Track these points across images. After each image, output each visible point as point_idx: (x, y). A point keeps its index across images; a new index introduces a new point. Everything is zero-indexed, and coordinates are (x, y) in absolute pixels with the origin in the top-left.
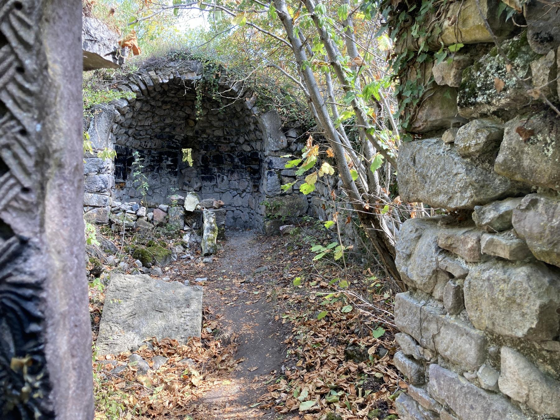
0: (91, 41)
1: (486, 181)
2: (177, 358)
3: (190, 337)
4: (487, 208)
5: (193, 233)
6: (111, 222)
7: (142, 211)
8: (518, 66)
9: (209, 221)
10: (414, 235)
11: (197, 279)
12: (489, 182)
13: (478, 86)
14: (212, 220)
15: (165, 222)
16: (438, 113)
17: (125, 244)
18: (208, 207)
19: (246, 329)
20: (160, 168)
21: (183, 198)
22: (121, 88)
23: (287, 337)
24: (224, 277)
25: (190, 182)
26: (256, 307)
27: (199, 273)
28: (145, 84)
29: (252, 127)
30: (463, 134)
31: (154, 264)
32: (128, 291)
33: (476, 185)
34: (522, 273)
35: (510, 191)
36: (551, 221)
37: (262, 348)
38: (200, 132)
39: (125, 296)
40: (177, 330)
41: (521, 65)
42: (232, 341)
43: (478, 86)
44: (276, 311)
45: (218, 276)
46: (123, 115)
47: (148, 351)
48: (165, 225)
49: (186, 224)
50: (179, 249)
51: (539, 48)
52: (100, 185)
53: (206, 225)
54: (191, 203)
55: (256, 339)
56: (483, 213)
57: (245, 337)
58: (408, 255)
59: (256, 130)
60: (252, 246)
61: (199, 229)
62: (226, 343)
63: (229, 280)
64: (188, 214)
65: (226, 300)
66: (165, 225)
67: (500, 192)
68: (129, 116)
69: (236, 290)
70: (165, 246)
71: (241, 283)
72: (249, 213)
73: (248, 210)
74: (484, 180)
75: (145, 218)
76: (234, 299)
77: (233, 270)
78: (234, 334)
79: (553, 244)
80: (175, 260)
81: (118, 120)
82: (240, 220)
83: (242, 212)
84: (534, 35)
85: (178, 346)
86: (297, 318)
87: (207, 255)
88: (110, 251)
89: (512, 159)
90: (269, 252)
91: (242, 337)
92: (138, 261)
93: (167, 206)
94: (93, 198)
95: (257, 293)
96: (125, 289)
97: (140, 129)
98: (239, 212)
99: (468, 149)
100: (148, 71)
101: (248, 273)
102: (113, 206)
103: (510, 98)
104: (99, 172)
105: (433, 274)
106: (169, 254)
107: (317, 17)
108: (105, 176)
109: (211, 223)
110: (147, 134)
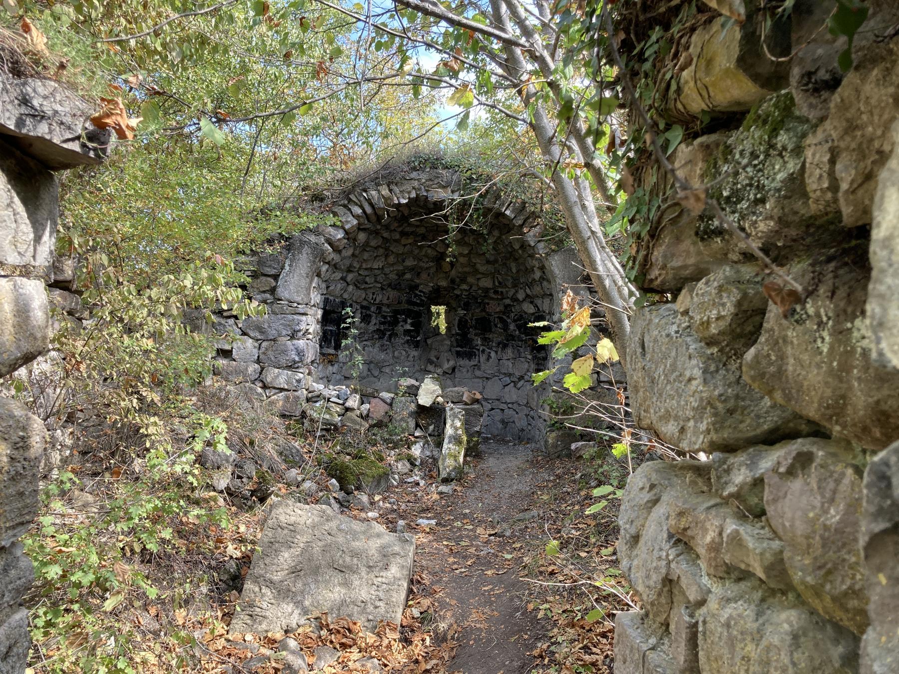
0: (34, 116)
1: (743, 399)
2: (355, 654)
3: (382, 621)
4: (740, 458)
5: (427, 442)
6: (304, 415)
7: (353, 402)
8: (784, 148)
9: (453, 426)
10: (646, 496)
11: (420, 521)
12: (748, 402)
13: (725, 194)
14: (458, 424)
15: (386, 420)
16: (688, 252)
17: (318, 451)
18: (455, 401)
19: (476, 619)
20: (394, 335)
21: (417, 384)
22: (336, 210)
23: (539, 645)
24: (465, 521)
25: (438, 359)
26: (501, 582)
27: (427, 510)
28: (371, 204)
29: (537, 275)
30: (703, 295)
31: (358, 488)
32: (294, 531)
33: (720, 406)
34: (786, 626)
35: (791, 425)
36: (826, 512)
37: (495, 659)
38: (458, 280)
39: (290, 539)
40: (363, 605)
41: (790, 147)
42: (449, 637)
43: (725, 194)
44: (531, 594)
45: (456, 519)
46: (336, 250)
47: (312, 635)
48: (386, 426)
49: (417, 425)
50: (402, 466)
51: (811, 106)
52: (293, 356)
53: (449, 431)
54: (429, 392)
55: (490, 641)
56: (728, 471)
57: (472, 633)
58: (633, 537)
59: (544, 279)
60: (521, 472)
61: (439, 436)
62: (440, 639)
63: (471, 527)
64: (422, 410)
65: (455, 563)
66: (386, 426)
67: (766, 427)
68: (348, 253)
69: (477, 546)
70: (381, 459)
71: (490, 535)
72: (527, 415)
73: (526, 411)
74: (737, 397)
75: (358, 412)
76: (469, 563)
77: (482, 512)
78: (455, 626)
79: (822, 572)
80: (395, 483)
81: (329, 258)
82: (513, 425)
83: (517, 413)
84: (803, 76)
85: (360, 634)
86: (563, 612)
87: (446, 481)
88: (292, 460)
89: (769, 355)
90: (547, 486)
91: (466, 633)
92: (334, 481)
93: (392, 395)
94: (281, 378)
95: (509, 557)
96: (291, 527)
97: (366, 273)
98: (511, 412)
99: (707, 328)
100: (378, 185)
101: (503, 520)
102: (311, 389)
103: (771, 218)
104: (292, 337)
105: (664, 586)
106: (385, 473)
107: (559, 85)
108: (301, 343)
109: (456, 429)
110: (376, 281)
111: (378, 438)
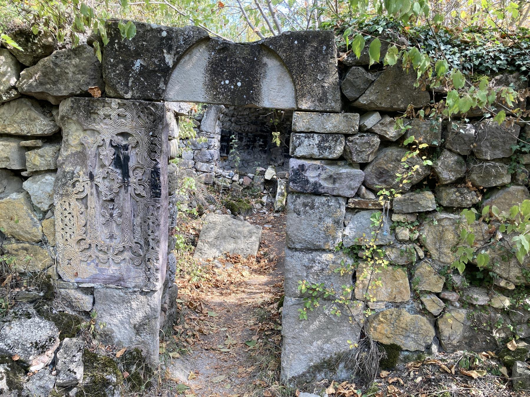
6: (214, 183)
7: (236, 178)
9: (281, 188)
14: (283, 187)
15: (251, 186)
20: (254, 147)
21: (265, 170)
27: (269, 222)
31: (239, 214)
38: (285, 120)
45: (280, 225)
48: (251, 189)
49: (265, 189)
50: (258, 206)
53: (279, 190)
54: (270, 173)
62: (270, 261)
64: (266, 181)
66: (251, 189)
68: (232, 108)
70: (249, 203)
81: (223, 111)
87: (277, 212)
88: (211, 201)
94: (204, 167)
97: (240, 117)
104: (208, 149)
108: (212, 151)
109: (282, 190)
110: (245, 121)
111: (247, 194)
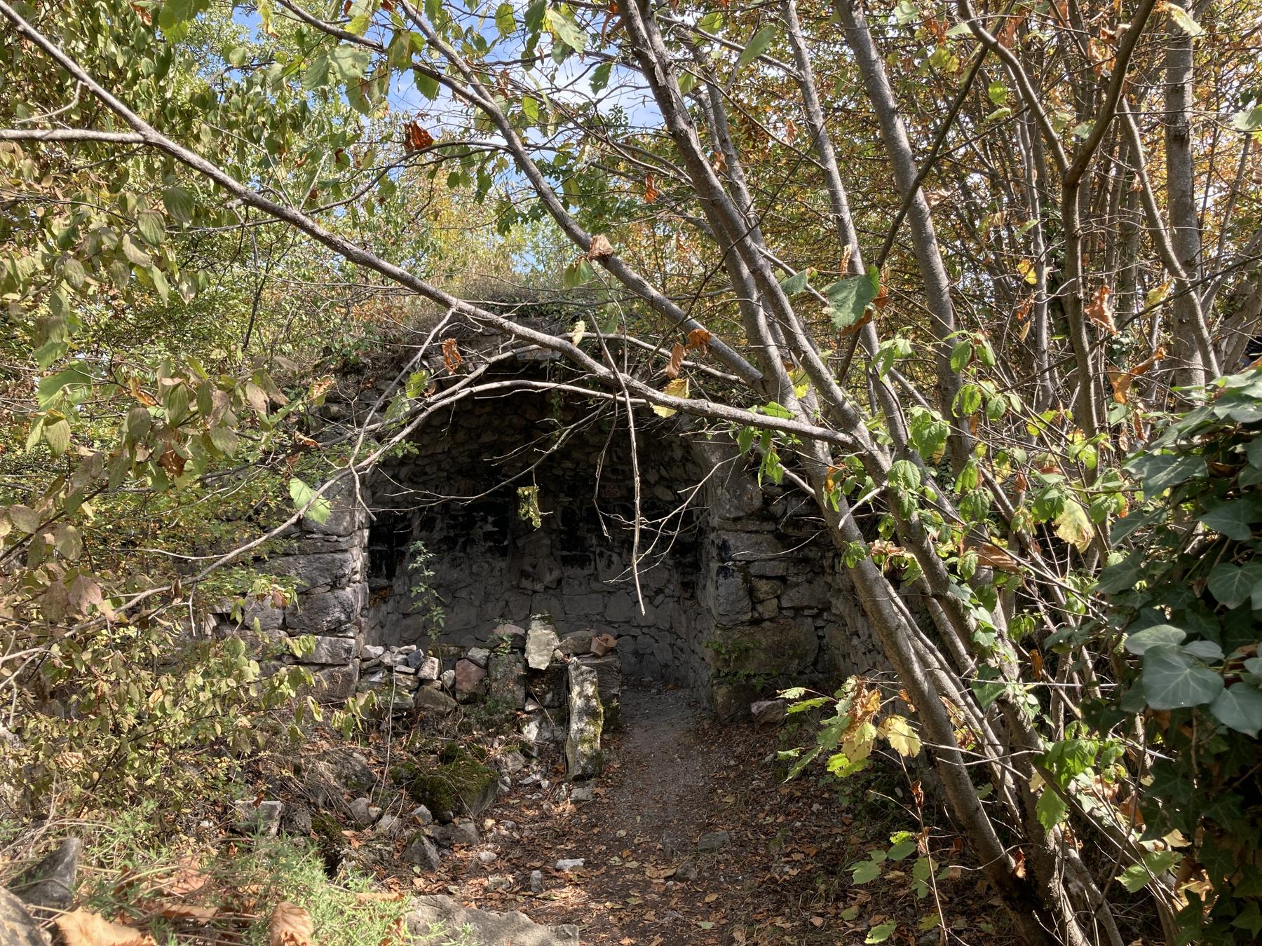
5: (545, 719)
7: (431, 669)
9: (582, 692)
14: (590, 690)
15: (481, 692)
20: (470, 542)
25: (534, 567)
29: (678, 454)
45: (611, 851)
50: (512, 763)
52: (337, 615)
53: (577, 702)
59: (687, 460)
72: (672, 645)
73: (669, 639)
80: (506, 789)
82: (652, 659)
83: (657, 641)
87: (581, 779)
92: (423, 808)
98: (648, 639)
109: (588, 698)
110: (439, 469)
111: (473, 720)
